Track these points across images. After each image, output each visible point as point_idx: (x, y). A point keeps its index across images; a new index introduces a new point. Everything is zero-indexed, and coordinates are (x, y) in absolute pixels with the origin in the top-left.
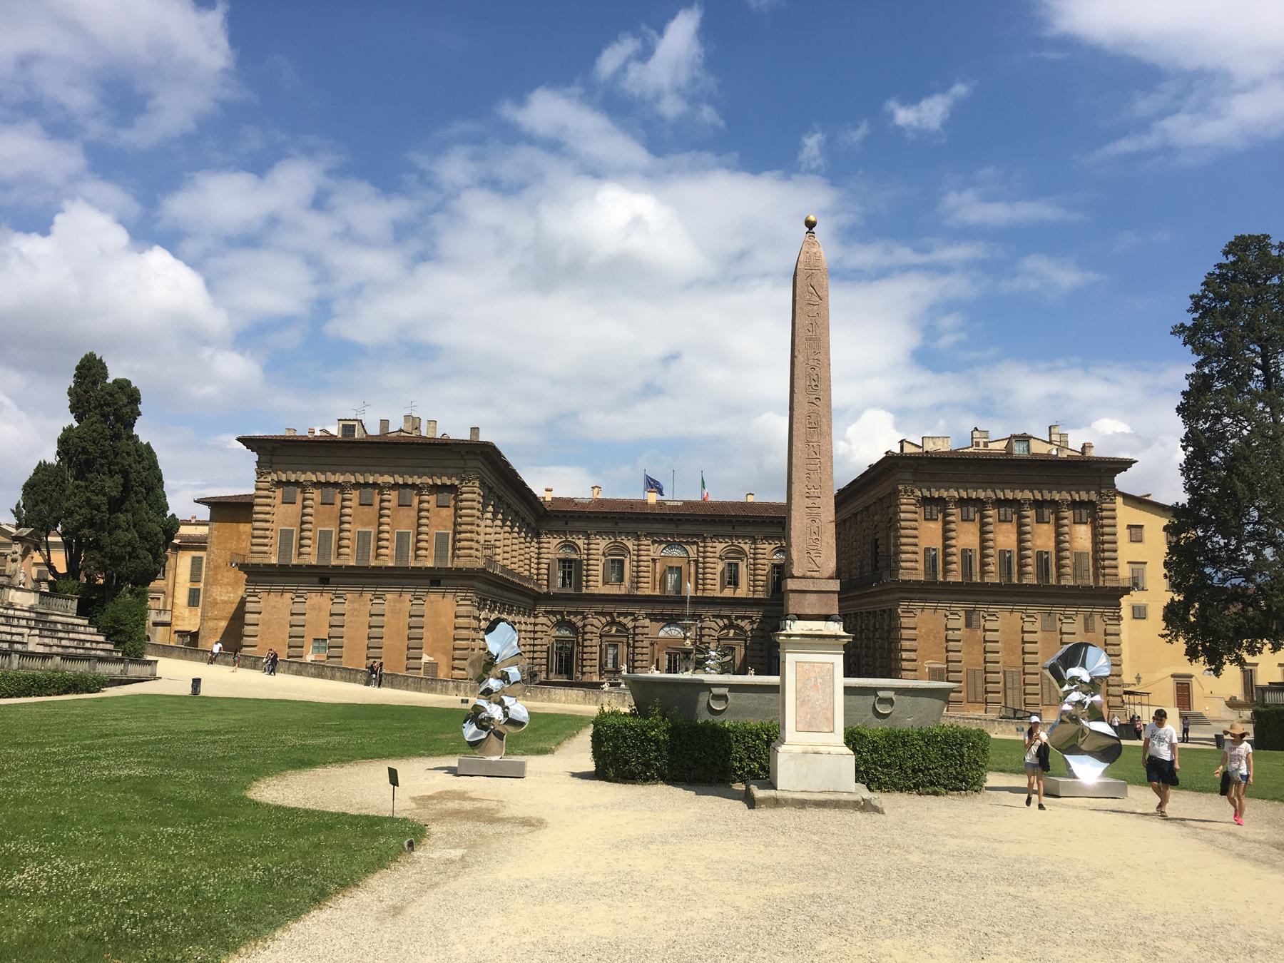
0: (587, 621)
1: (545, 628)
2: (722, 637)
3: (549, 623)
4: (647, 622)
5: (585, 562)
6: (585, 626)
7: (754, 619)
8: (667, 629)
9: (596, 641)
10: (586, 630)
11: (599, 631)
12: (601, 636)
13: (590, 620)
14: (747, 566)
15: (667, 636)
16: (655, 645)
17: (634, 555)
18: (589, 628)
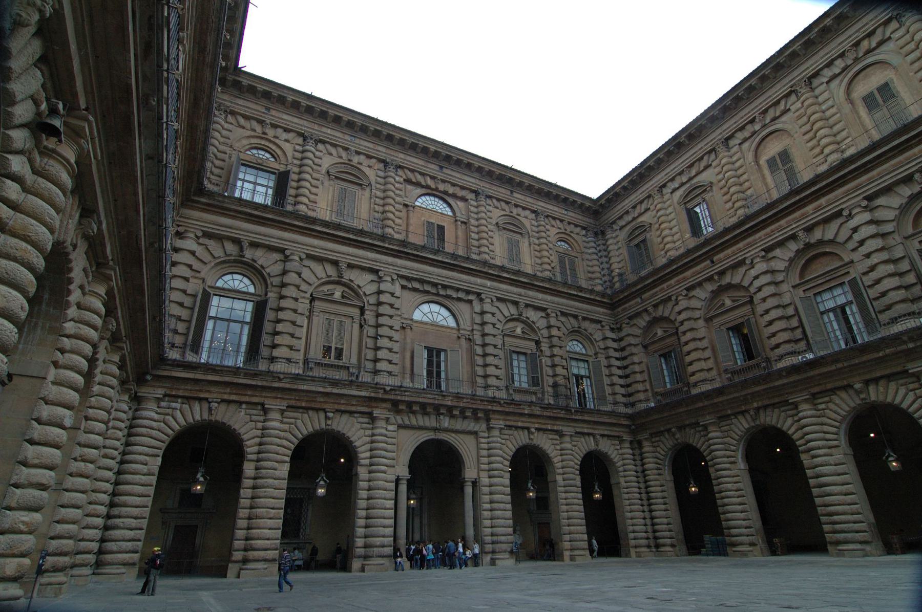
0: (289, 266)
1: (196, 265)
2: (507, 332)
3: (207, 257)
4: (398, 291)
5: (294, 177)
6: (284, 273)
7: (549, 311)
8: (425, 308)
9: (303, 306)
10: (287, 279)
11: (310, 290)
12: (313, 299)
13: (292, 265)
14: (530, 245)
15: (425, 319)
16: (408, 331)
17: (377, 189)
18: (292, 278)
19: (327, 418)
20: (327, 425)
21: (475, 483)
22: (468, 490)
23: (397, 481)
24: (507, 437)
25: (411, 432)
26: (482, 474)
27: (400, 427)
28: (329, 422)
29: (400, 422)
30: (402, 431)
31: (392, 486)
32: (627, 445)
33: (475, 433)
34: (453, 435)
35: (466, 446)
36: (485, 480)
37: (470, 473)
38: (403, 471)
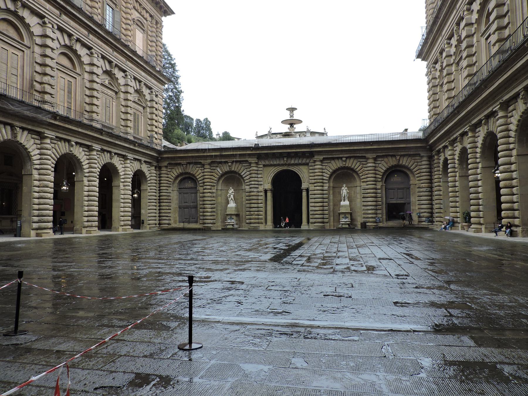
19: (229, 166)
20: (230, 169)
21: (307, 190)
22: (304, 194)
23: (266, 191)
24: (326, 164)
25: (271, 168)
26: (310, 185)
27: (264, 166)
28: (231, 168)
29: (263, 163)
30: (266, 168)
31: (263, 194)
32: (425, 159)
33: (307, 164)
34: (295, 167)
35: (303, 173)
36: (311, 187)
37: (304, 186)
38: (268, 186)
